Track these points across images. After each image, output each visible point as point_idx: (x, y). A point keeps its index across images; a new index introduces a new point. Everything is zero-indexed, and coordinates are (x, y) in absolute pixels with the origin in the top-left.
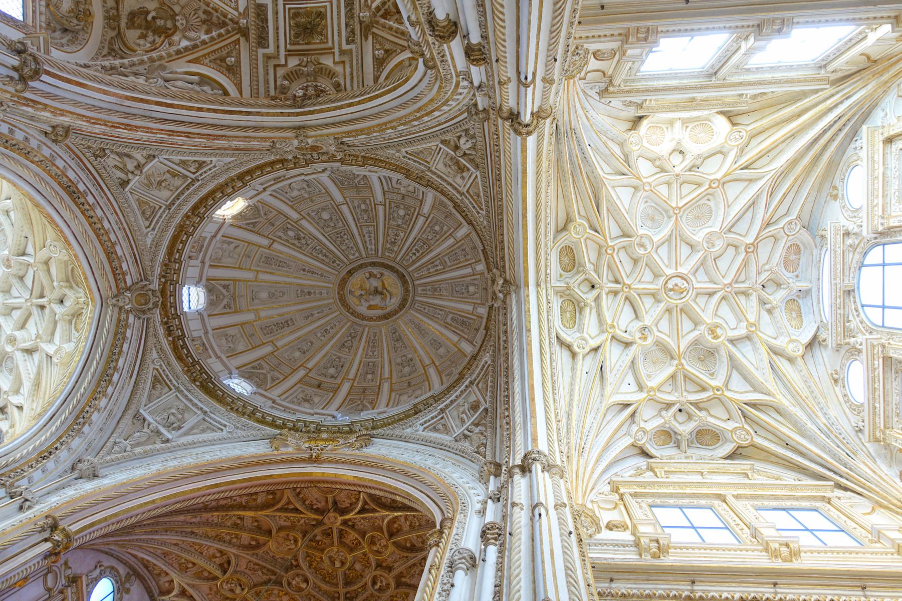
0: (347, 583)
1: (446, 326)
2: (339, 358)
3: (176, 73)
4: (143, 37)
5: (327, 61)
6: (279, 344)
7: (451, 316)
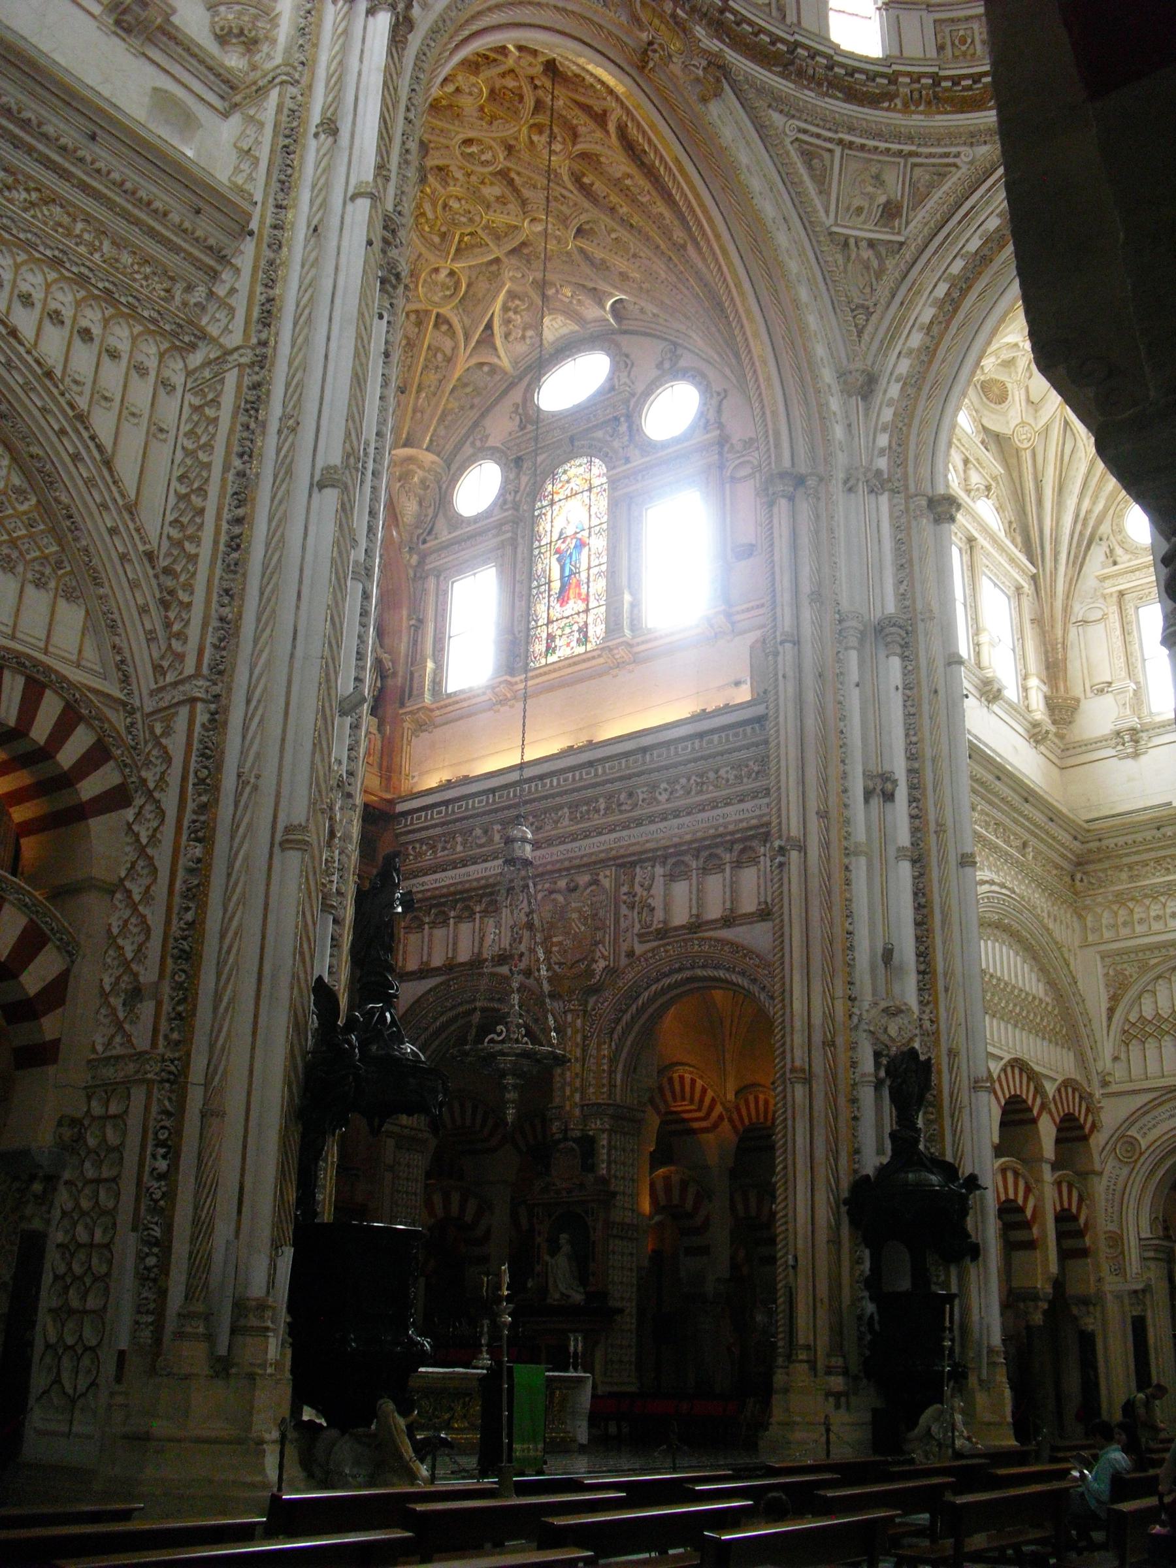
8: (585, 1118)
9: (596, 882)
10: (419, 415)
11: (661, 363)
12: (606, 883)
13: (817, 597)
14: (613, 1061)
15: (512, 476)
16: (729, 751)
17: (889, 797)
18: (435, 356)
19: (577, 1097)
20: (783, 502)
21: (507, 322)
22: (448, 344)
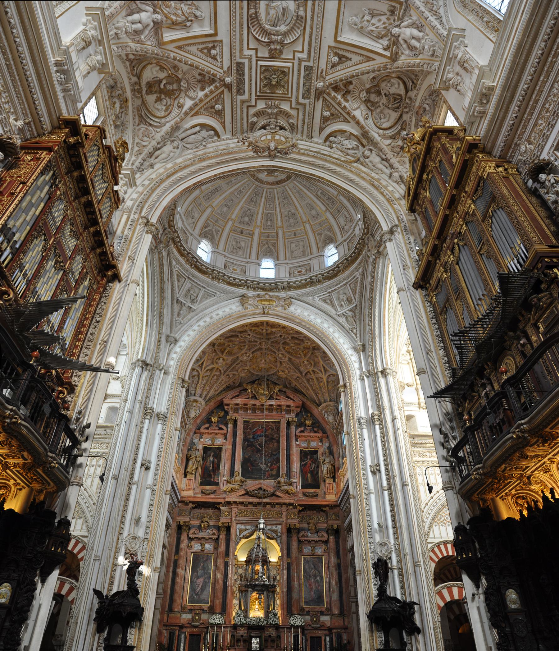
0: (267, 334)
1: (317, 197)
2: (250, 210)
3: (187, 130)
4: (159, 100)
5: (285, 106)
6: (214, 205)
7: (320, 191)
17: (379, 471)
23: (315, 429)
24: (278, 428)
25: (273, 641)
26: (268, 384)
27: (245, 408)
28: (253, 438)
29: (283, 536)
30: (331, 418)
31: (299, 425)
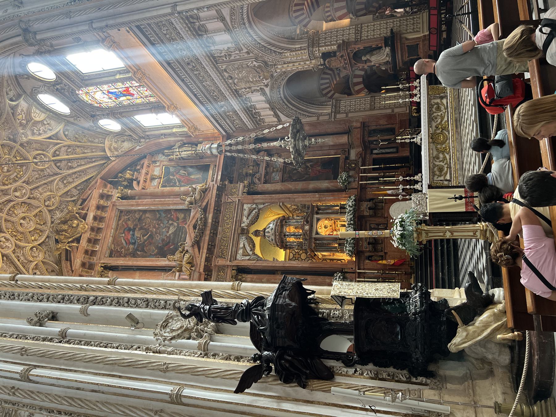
8: (315, 58)
9: (225, 70)
10: (93, 150)
11: (26, 78)
12: (224, 67)
13: (68, 14)
14: (291, 50)
15: (99, 118)
16: (155, 32)
18: (70, 152)
19: (308, 63)
20: (38, 37)
21: (45, 132)
22: (63, 149)
23: (138, 167)
24: (129, 212)
25: (376, 206)
26: (65, 222)
27: (90, 253)
28: (134, 244)
29: (255, 201)
30: (127, 145)
31: (130, 186)
